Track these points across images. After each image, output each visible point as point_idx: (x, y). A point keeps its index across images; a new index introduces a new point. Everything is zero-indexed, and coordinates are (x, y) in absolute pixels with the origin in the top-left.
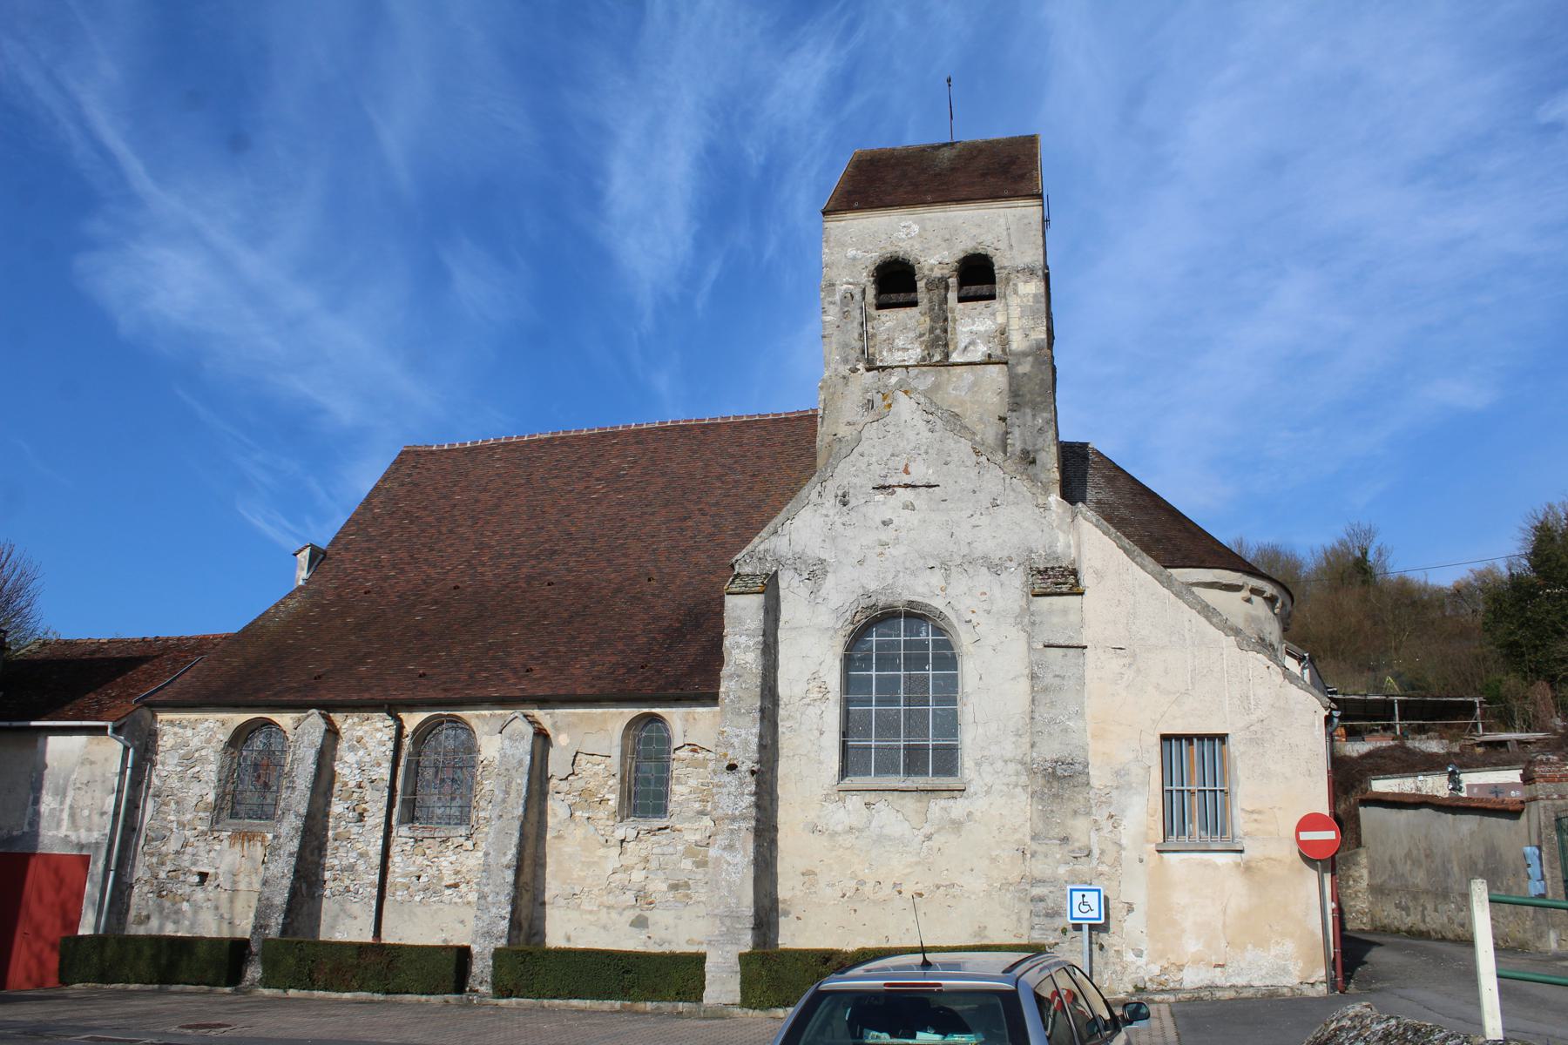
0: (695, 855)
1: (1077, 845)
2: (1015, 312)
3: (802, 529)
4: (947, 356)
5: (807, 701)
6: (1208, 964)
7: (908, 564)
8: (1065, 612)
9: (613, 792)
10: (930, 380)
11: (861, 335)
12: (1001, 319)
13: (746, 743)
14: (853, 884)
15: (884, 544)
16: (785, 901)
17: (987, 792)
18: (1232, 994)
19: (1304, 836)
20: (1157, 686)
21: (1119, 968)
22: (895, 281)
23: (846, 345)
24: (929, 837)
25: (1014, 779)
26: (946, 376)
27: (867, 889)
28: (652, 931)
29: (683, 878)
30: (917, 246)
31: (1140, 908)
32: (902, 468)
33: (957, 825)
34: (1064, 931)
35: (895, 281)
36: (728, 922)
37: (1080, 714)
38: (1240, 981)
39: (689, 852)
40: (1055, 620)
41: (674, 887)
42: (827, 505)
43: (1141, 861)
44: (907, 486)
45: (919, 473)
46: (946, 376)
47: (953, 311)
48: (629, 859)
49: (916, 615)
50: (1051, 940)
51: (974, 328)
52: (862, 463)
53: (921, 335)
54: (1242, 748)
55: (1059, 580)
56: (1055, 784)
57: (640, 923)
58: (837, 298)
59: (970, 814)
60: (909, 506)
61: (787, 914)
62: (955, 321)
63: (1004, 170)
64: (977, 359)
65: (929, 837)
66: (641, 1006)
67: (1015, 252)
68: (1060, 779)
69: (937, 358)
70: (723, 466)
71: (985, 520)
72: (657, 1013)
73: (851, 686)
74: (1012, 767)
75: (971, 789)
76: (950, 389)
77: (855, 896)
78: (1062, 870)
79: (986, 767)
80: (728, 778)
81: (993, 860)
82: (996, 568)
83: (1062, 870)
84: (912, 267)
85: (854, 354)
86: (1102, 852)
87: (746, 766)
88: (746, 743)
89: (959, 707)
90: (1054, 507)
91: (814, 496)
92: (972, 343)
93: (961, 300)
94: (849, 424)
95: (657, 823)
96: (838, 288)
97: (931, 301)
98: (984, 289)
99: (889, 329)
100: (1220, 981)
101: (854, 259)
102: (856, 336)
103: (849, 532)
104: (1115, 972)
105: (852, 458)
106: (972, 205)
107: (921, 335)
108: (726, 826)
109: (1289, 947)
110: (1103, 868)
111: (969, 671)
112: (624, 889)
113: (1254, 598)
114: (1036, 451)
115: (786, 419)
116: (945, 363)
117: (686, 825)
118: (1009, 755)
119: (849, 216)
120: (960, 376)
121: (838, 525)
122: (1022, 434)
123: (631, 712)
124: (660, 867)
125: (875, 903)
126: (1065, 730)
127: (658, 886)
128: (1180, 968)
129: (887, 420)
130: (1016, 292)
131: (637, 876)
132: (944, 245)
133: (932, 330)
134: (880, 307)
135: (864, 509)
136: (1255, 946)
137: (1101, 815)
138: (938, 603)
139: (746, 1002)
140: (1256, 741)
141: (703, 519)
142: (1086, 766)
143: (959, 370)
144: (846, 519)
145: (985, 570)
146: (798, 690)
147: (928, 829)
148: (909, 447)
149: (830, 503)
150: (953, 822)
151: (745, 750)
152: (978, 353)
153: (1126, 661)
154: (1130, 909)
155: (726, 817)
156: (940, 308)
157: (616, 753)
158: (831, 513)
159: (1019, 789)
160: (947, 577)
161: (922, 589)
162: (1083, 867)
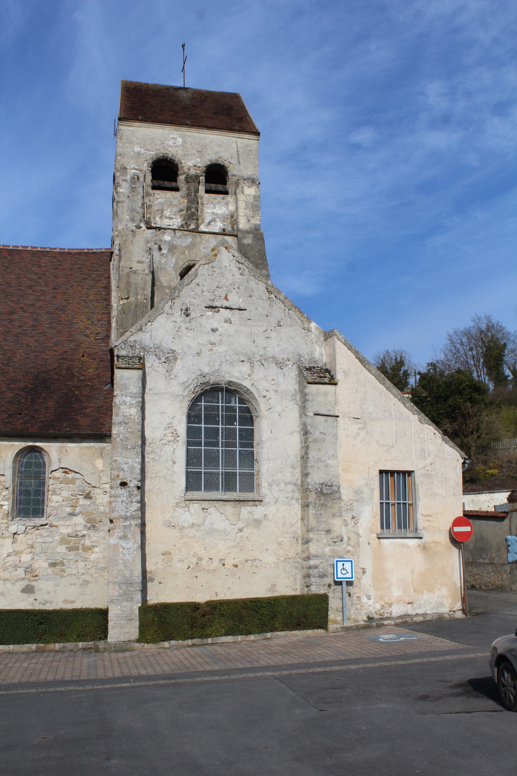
0: (68, 543)
1: (335, 534)
2: (242, 205)
3: (160, 330)
4: (198, 226)
5: (164, 441)
6: (405, 602)
8: (326, 394)
9: (7, 500)
11: (143, 204)
12: (232, 208)
13: (132, 468)
14: (195, 560)
15: (213, 344)
16: (151, 572)
17: (276, 502)
18: (421, 619)
19: (457, 529)
20: (377, 442)
21: (359, 607)
22: (164, 172)
23: (133, 210)
24: (241, 530)
25: (291, 494)
26: (199, 239)
27: (204, 563)
28: (37, 595)
29: (59, 558)
30: (180, 152)
31: (369, 571)
32: (223, 297)
33: (258, 523)
34: (329, 586)
35: (164, 172)
36: (124, 587)
37: (334, 456)
38: (421, 611)
39: (63, 541)
40: (320, 399)
41: (53, 565)
42: (176, 314)
43: (369, 544)
44: (226, 308)
45: (234, 300)
46: (199, 239)
47: (202, 198)
48: (20, 546)
49: (231, 391)
51: (215, 211)
52: (198, 290)
53: (181, 211)
54: (421, 479)
55: (325, 376)
56: (322, 498)
57: (29, 590)
58: (128, 177)
59: (265, 516)
60: (228, 321)
61: (152, 580)
62: (203, 204)
63: (225, 113)
64: (217, 231)
65: (241, 530)
66: (51, 646)
67: (242, 167)
68: (320, 496)
69: (192, 227)
70: (31, 280)
71: (273, 334)
72: (62, 651)
74: (290, 487)
75: (266, 501)
76: (201, 248)
77: (196, 568)
79: (274, 487)
80: (121, 491)
81: (280, 544)
82: (280, 365)
83: (327, 550)
84: (176, 166)
85: (138, 217)
86: (349, 539)
87: (133, 483)
88: (132, 468)
89: (255, 450)
90: (313, 330)
91: (167, 308)
92: (214, 220)
93: (207, 191)
94: (139, 262)
95: (38, 521)
96: (129, 171)
97: (188, 189)
98: (220, 187)
99: (160, 203)
101: (139, 153)
102: (140, 205)
103: (190, 334)
104: (357, 609)
106: (216, 132)
107: (181, 211)
108: (121, 523)
109: (444, 591)
110: (350, 548)
111: (264, 429)
112: (16, 567)
115: (69, 253)
116: (195, 231)
117: (61, 523)
118: (288, 480)
119: (137, 124)
121: (183, 328)
123: (19, 445)
124: (43, 552)
125: (209, 571)
126: (327, 466)
127: (41, 564)
128: (390, 605)
129: (214, 264)
130: (243, 192)
131: (26, 558)
132: (198, 154)
133: (188, 209)
134: (154, 188)
135: (200, 320)
136: (428, 591)
137: (348, 516)
138: (246, 383)
139: (142, 638)
140: (428, 476)
141: (25, 314)
142: (339, 488)
143: (207, 236)
145: (273, 365)
146: (158, 434)
147: (240, 525)
148: (228, 283)
150: (255, 520)
151: (132, 472)
152: (218, 227)
153: (361, 426)
154: (364, 572)
155: (121, 517)
156: (195, 195)
157: (9, 473)
158: (179, 320)
160: (252, 367)
161: (236, 374)
162: (340, 548)
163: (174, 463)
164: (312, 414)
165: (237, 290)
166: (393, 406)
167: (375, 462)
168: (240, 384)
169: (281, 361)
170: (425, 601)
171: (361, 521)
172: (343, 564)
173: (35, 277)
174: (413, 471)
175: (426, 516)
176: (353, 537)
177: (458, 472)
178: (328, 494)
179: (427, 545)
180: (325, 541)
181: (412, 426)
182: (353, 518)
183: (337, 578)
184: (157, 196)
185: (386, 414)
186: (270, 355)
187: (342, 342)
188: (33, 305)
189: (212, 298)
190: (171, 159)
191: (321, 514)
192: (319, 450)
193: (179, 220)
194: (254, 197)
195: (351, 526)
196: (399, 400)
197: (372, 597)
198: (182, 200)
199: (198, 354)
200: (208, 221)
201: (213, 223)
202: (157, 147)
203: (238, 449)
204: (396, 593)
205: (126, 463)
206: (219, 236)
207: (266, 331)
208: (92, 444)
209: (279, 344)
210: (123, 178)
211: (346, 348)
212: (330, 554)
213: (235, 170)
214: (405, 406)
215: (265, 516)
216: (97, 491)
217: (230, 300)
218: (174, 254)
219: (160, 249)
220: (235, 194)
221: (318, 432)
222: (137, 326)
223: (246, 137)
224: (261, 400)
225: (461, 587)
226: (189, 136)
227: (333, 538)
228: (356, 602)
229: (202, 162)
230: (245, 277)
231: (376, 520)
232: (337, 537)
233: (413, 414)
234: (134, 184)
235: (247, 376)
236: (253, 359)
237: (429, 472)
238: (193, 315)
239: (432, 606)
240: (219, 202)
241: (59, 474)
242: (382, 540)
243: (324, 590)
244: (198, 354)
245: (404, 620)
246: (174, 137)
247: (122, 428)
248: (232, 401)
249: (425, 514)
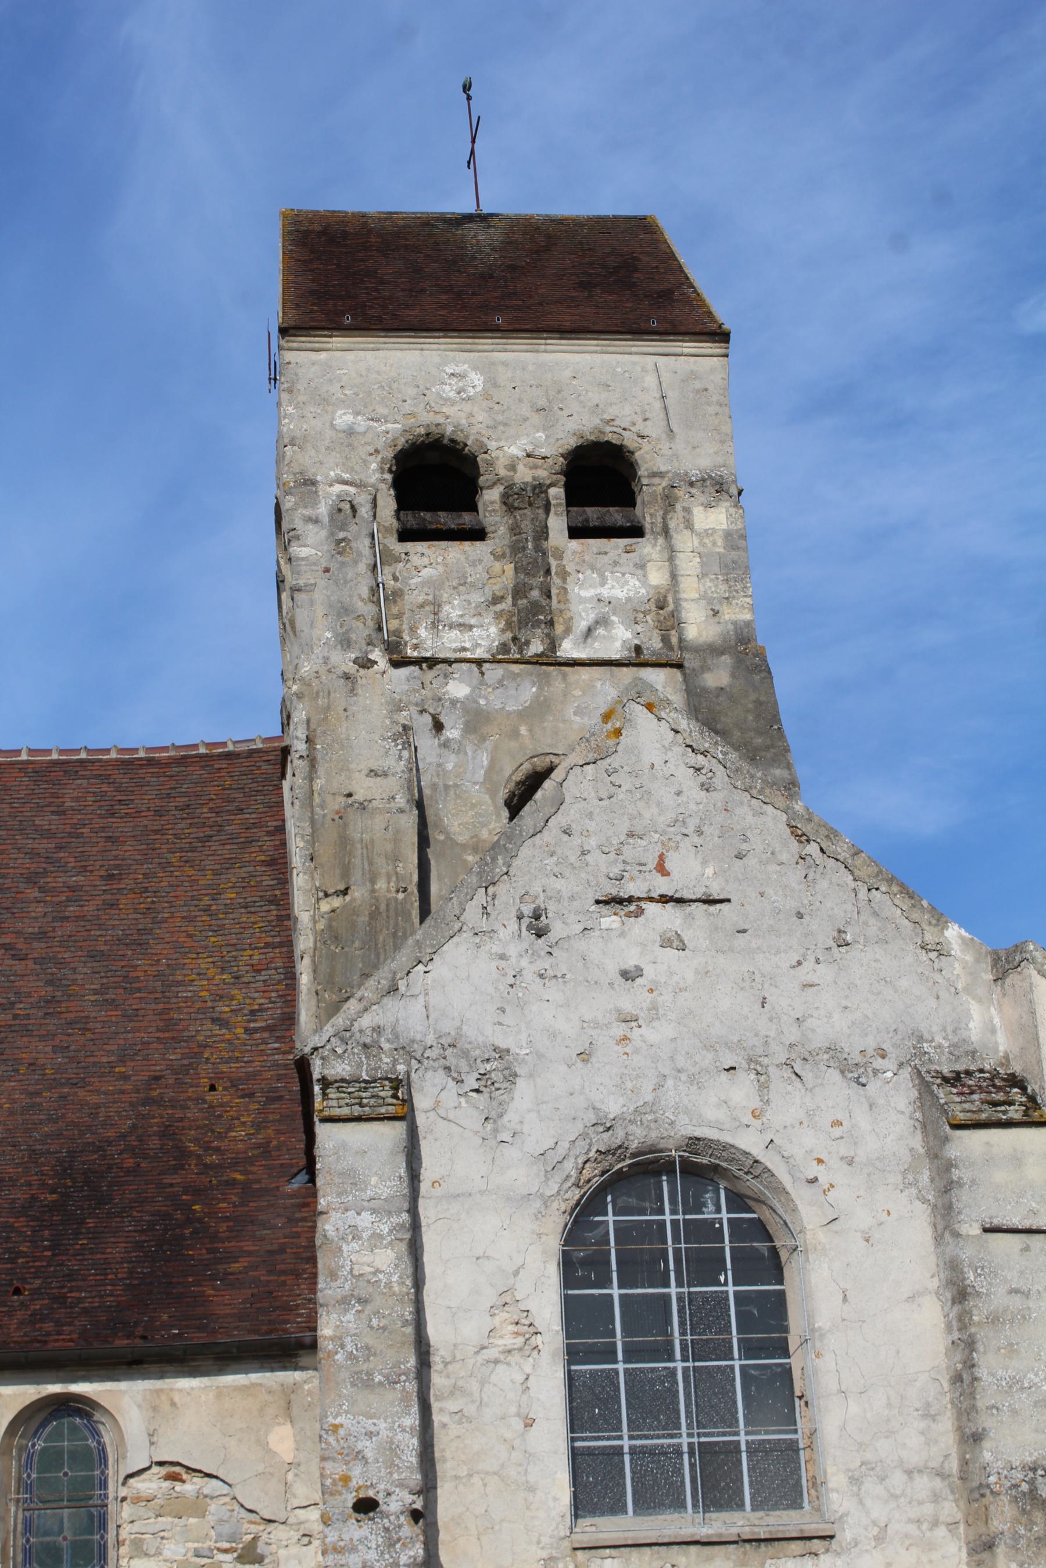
2: (689, 565)
3: (455, 986)
4: (553, 645)
5: (492, 1353)
7: (681, 1061)
8: (1017, 1160)
11: (374, 590)
12: (657, 577)
13: (392, 1449)
15: (629, 1020)
17: (880, 1539)
22: (435, 483)
23: (343, 611)
25: (928, 1509)
30: (481, 416)
32: (652, 864)
35: (435, 483)
40: (1000, 1176)
42: (503, 933)
44: (664, 899)
45: (689, 872)
47: (559, 555)
49: (699, 1169)
51: (605, 592)
52: (570, 848)
53: (496, 600)
58: (323, 510)
60: (673, 942)
62: (564, 575)
63: (614, 280)
67: (679, 445)
69: (536, 647)
70: (33, 854)
71: (824, 974)
73: (582, 1320)
74: (924, 1485)
75: (846, 1535)
79: (870, 1485)
80: (358, 1530)
82: (856, 1072)
84: (471, 461)
85: (361, 631)
87: (397, 1503)
88: (392, 1449)
89: (795, 1362)
90: (956, 949)
91: (472, 913)
92: (602, 621)
93: (576, 532)
94: (373, 773)
98: (616, 516)
99: (428, 583)
101: (350, 432)
102: (365, 592)
103: (553, 992)
105: (547, 836)
106: (591, 344)
107: (496, 600)
111: (821, 1289)
115: (150, 762)
116: (549, 660)
118: (915, 1460)
119: (338, 341)
120: (588, 688)
121: (529, 975)
129: (615, 761)
130: (689, 525)
132: (536, 419)
133: (519, 591)
134: (406, 535)
135: (581, 945)
138: (750, 1142)
141: (19, 967)
143: (585, 674)
144: (545, 963)
145: (834, 1075)
148: (662, 820)
149: (509, 935)
152: (617, 640)
156: (538, 548)
158: (513, 950)
159: (942, 1531)
160: (763, 1087)
161: (712, 1112)
163: (529, 1423)
164: (976, 1230)
165: (697, 840)
168: (726, 1147)
169: (858, 1058)
173: (45, 846)
184: (415, 560)
186: (818, 1041)
188: (42, 935)
189: (615, 871)
190: (452, 441)
192: (1012, 1349)
193: (493, 630)
194: (728, 535)
198: (497, 566)
199: (585, 1056)
200: (582, 625)
201: (601, 631)
202: (407, 408)
203: (737, 1364)
205: (370, 1435)
206: (625, 669)
207: (799, 963)
208: (254, 1377)
209: (844, 1003)
210: (307, 512)
213: (656, 459)
216: (279, 1533)
218: (483, 739)
219: (438, 727)
220: (666, 532)
221: (1002, 1290)
222: (381, 978)
223: (686, 351)
224: (802, 1196)
226: (505, 364)
229: (552, 440)
230: (718, 796)
234: (342, 529)
235: (747, 1119)
236: (765, 1061)
238: (557, 930)
240: (616, 563)
241: (150, 1485)
244: (585, 1056)
246: (457, 370)
247: (350, 1316)
248: (704, 1205)
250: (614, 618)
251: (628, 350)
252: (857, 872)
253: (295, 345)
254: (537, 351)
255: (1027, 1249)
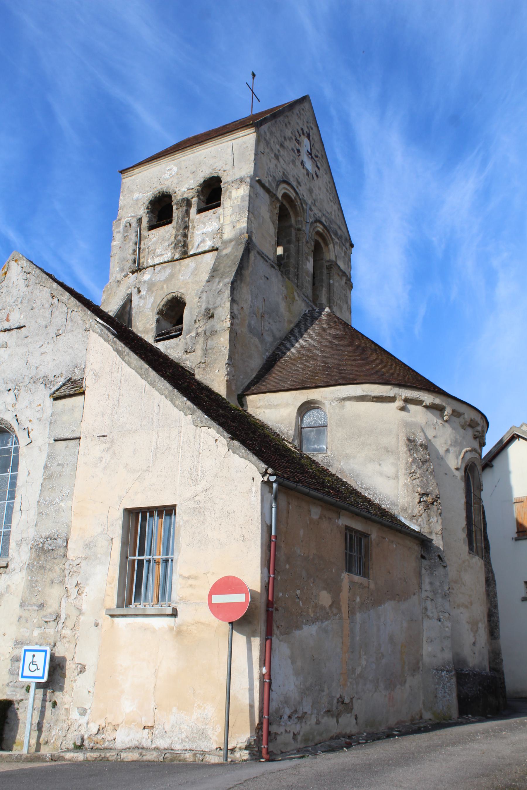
1: (50, 610)
8: (72, 410)
10: (168, 271)
11: (135, 251)
18: (133, 756)
19: (217, 599)
22: (161, 209)
32: (5, 317)
38: (163, 743)
43: (97, 625)
46: (178, 267)
47: (193, 220)
50: (19, 697)
51: (205, 230)
56: (43, 557)
58: (121, 228)
59: (8, 587)
75: (11, 567)
78: (36, 633)
100: (146, 743)
101: (137, 200)
102: (131, 251)
113: (410, 407)
114: (215, 308)
122: (207, 297)
130: (230, 198)
132: (191, 176)
137: (70, 583)
140: (197, 511)
153: (106, 446)
165: (20, 306)
166: (156, 409)
167: (120, 497)
169: (52, 378)
170: (173, 725)
171: (86, 590)
172: (34, 656)
174: (174, 507)
175: (188, 578)
176: (74, 613)
177: (253, 499)
178: (49, 550)
179: (184, 628)
180: (35, 621)
181: (182, 434)
182: (77, 584)
183: (43, 677)
185: (144, 423)
187: (97, 333)
190: (166, 192)
191: (37, 581)
193: (170, 254)
195: (72, 597)
196: (166, 397)
197: (89, 711)
201: (202, 245)
203: (6, 502)
204: (128, 707)
206: (199, 256)
207: (42, 345)
209: (54, 358)
210: (117, 230)
211: (102, 340)
212: (37, 641)
214: (174, 404)
215: (8, 587)
217: (11, 321)
218: (153, 292)
219: (139, 291)
223: (241, 135)
225: (251, 706)
226: (184, 161)
227: (45, 616)
228: (62, 717)
229: (195, 182)
231: (112, 588)
232: (51, 614)
233: (186, 415)
234: (126, 232)
235: (10, 408)
236: (21, 385)
237: (201, 505)
239: (183, 736)
240: (210, 219)
242: (116, 620)
243: (21, 695)
245: (103, 755)
246: (170, 168)
248: (8, 443)
249: (186, 575)
250: (207, 239)
251: (222, 141)
252: (68, 306)
253: (125, 176)
254: (194, 153)
255: (67, 447)
